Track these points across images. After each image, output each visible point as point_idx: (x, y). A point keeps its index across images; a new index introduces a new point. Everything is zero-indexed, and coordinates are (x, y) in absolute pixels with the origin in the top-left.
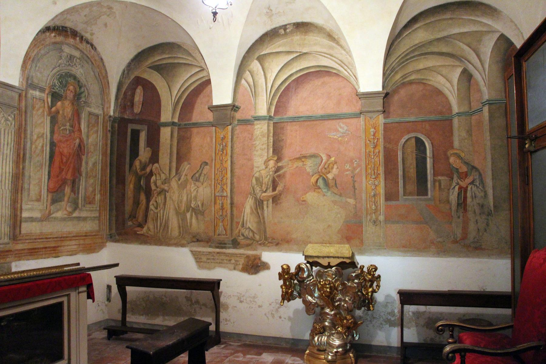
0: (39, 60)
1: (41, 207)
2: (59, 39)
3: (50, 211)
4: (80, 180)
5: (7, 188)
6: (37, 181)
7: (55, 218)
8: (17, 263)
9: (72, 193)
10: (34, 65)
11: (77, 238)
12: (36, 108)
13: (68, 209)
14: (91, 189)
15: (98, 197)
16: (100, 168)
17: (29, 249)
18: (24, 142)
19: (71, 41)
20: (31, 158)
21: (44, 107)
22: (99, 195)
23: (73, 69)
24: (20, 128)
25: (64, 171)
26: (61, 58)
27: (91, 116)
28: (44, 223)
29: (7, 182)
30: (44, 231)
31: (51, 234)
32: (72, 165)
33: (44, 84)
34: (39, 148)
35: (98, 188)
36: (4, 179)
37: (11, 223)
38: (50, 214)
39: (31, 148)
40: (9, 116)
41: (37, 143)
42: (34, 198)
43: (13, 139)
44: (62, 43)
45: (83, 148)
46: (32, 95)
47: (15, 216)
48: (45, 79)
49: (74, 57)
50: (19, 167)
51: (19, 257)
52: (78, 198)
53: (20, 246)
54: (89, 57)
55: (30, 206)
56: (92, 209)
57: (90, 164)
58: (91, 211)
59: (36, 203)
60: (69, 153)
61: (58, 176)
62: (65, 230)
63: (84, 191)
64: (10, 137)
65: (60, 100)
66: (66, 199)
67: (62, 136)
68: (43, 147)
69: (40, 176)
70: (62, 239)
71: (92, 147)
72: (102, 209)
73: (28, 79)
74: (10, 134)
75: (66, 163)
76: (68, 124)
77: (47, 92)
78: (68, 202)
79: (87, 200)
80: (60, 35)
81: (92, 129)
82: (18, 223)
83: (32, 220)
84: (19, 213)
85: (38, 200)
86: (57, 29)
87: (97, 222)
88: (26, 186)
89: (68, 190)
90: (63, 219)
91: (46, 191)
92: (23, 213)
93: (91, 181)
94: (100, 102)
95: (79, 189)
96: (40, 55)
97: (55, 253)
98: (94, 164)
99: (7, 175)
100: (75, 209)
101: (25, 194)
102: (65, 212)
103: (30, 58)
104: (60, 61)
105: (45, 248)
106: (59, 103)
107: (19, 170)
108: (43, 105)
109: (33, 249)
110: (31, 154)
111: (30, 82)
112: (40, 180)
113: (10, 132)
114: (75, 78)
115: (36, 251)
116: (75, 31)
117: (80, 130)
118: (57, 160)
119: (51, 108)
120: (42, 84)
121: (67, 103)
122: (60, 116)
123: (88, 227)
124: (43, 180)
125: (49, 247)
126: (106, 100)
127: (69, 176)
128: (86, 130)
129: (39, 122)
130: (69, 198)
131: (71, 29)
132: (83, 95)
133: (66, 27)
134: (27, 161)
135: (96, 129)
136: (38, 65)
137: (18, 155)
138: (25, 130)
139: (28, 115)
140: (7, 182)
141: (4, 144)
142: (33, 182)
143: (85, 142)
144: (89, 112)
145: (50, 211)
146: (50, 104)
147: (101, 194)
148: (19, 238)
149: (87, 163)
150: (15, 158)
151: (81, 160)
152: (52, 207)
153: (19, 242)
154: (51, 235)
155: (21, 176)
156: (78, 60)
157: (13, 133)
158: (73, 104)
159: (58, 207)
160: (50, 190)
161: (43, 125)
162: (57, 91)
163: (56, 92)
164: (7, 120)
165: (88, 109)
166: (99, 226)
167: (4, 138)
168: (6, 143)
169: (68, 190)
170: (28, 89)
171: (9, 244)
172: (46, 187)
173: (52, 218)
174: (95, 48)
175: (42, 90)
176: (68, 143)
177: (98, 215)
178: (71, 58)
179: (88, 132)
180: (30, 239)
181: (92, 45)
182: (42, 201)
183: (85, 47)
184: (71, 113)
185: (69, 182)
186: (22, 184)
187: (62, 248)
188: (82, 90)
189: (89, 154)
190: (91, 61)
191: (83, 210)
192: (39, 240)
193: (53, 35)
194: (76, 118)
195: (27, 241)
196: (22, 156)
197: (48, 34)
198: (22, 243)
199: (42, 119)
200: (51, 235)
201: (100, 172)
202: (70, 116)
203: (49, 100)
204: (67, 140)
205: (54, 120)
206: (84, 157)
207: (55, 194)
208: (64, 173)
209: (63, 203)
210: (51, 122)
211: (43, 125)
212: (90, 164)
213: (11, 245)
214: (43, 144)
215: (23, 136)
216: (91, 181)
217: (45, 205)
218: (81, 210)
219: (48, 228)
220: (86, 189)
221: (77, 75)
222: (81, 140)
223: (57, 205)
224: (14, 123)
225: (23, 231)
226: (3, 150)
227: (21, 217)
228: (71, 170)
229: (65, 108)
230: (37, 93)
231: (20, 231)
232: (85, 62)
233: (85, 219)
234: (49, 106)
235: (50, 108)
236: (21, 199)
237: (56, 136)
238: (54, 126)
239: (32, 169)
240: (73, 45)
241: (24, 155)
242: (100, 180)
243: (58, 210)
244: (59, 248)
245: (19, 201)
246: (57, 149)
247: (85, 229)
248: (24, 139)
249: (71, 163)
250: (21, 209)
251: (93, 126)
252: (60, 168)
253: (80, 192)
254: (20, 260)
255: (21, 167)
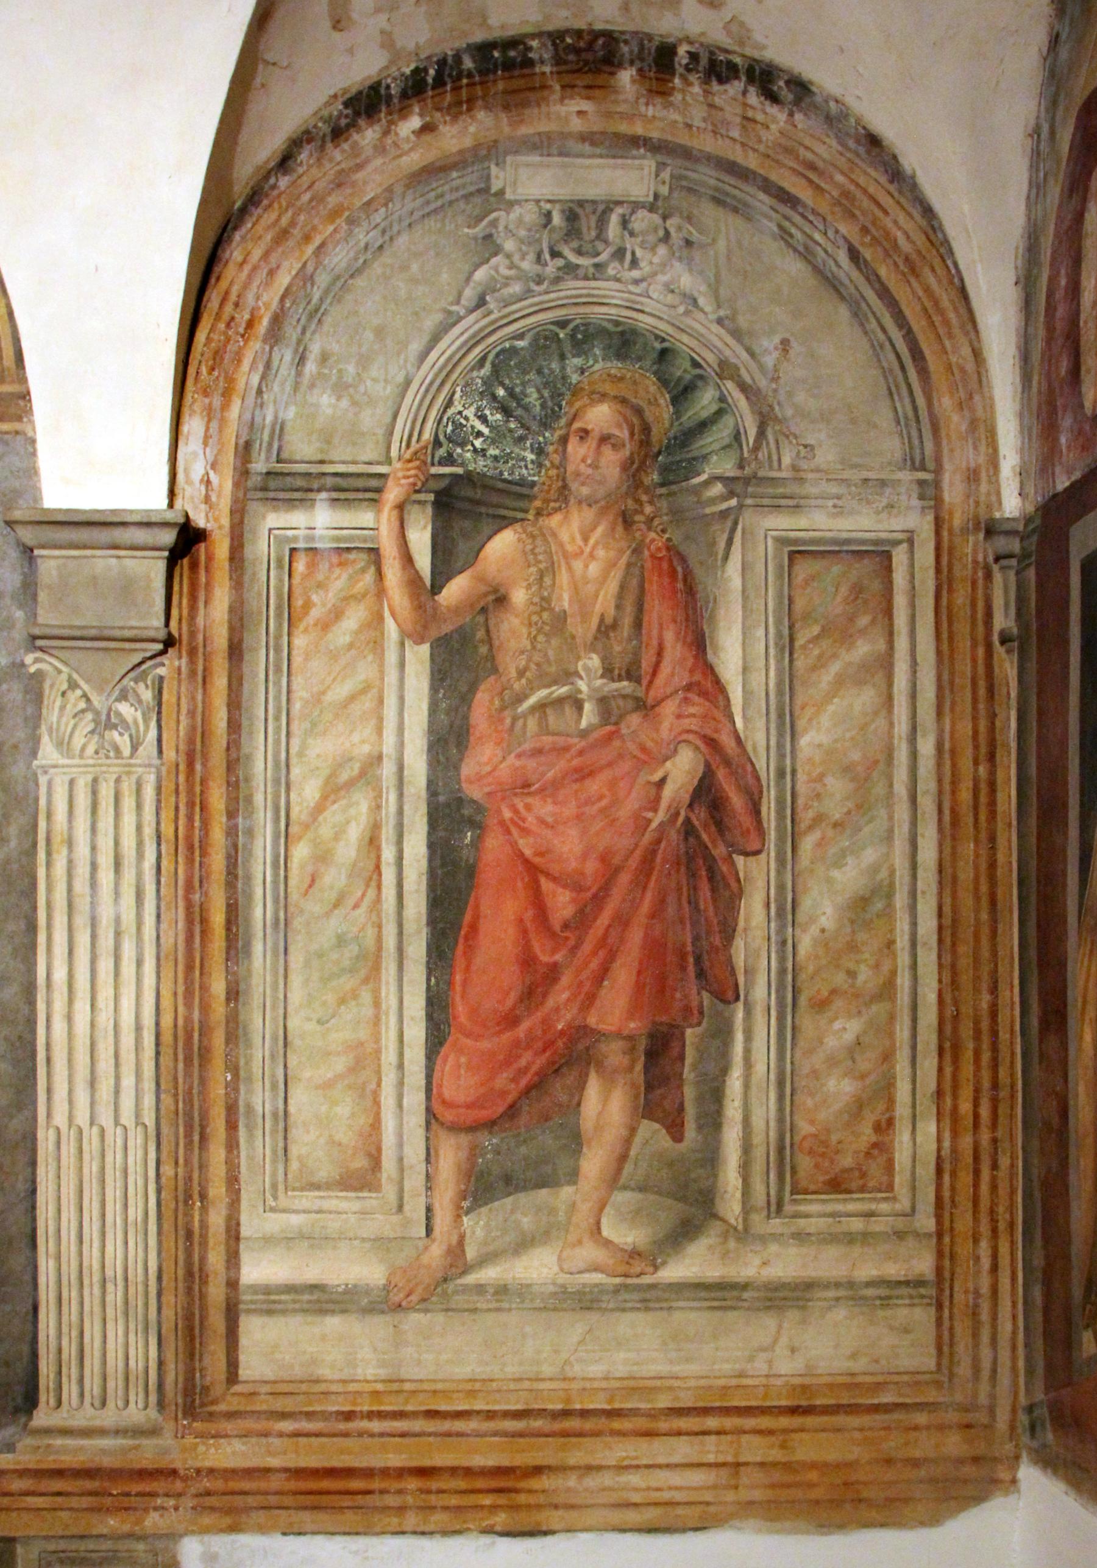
0: (316, 315)
1: (383, 1224)
2: (455, 136)
3: (457, 1250)
4: (722, 1033)
5: (127, 1117)
6: (340, 1064)
7: (502, 1290)
8: (221, 1543)
9: (648, 1128)
10: (285, 356)
11: (712, 1423)
12: (315, 613)
13: (605, 1233)
14: (840, 1088)
15: (917, 1142)
16: (928, 925)
17: (298, 1473)
18: (232, 832)
19: (570, 112)
20: (283, 924)
21: (381, 592)
22: (929, 1128)
23: (602, 287)
24: (194, 753)
25: (586, 982)
26: (489, 245)
27: (804, 569)
28: (415, 1318)
29: (128, 1081)
30: (410, 1372)
31: (473, 1387)
32: (636, 937)
33: (370, 451)
34: (348, 849)
35: (914, 1079)
36: (105, 1065)
37: (168, 1313)
38: (457, 1261)
39: (281, 863)
40: (123, 697)
41: (325, 831)
42: (325, 1172)
43: (149, 831)
44: (487, 152)
45: (737, 801)
46: (282, 541)
47: (194, 1277)
48: (371, 419)
49: (610, 205)
50: (204, 988)
51: (229, 1511)
52: (711, 1158)
53: (230, 1452)
54: (752, 162)
55: (295, 1220)
56: (857, 1225)
57: (822, 912)
58: (865, 1238)
59: (345, 1203)
60: (604, 859)
61: (511, 1020)
62: (596, 1370)
63: (765, 1112)
64: (129, 820)
65: (504, 522)
66: (593, 1163)
67: (538, 752)
68: (373, 842)
69: (363, 1034)
70: (574, 1424)
71: (837, 786)
72: (964, 1223)
73: (245, 451)
74: (128, 803)
75: (582, 920)
76: (594, 661)
77: (393, 494)
78: (613, 1180)
79: (805, 1163)
80: (461, 108)
81: (820, 664)
82: (217, 1321)
83: (319, 1300)
84: (216, 1259)
85: (361, 1178)
86: (439, 82)
87: (922, 1317)
88: (259, 1098)
89: (604, 1106)
90: (585, 1301)
91: (415, 1119)
92: (245, 1257)
93: (844, 1029)
94: (892, 446)
95: (714, 1095)
96: (323, 279)
97: (515, 1508)
98: (867, 907)
99: (128, 1040)
100: (683, 1233)
101: (257, 1147)
102: (589, 1252)
103: (250, 324)
104: (480, 275)
105: (423, 1472)
106: (502, 545)
107: (205, 1008)
108: (369, 577)
109: (331, 1472)
110: (283, 901)
111: (259, 465)
112: (364, 1059)
113: (127, 787)
114: (623, 341)
115: (356, 1484)
116: (596, 35)
117: (708, 686)
118: (499, 918)
119: (436, 588)
120: (353, 457)
121: (568, 528)
122: (512, 631)
123: (823, 1347)
124: (389, 1057)
125: (468, 1472)
126: (955, 422)
127: (615, 1010)
128: (766, 678)
129: (341, 691)
130: (623, 1158)
131: (556, 37)
132: (721, 433)
133: (513, 43)
134: (258, 948)
135: (863, 649)
136: (315, 349)
137: (196, 919)
138: (235, 762)
139: (257, 662)
140: (128, 1081)
141: (94, 866)
142: (308, 1074)
143: (763, 763)
144: (781, 541)
145: (457, 1250)
146: (424, 562)
147: (950, 1119)
148: (222, 1407)
149: (786, 909)
150: (174, 934)
151: (727, 893)
152: (478, 1227)
153: (228, 1426)
154: (471, 1394)
155: (218, 1040)
156: (642, 220)
157: (149, 792)
158: (627, 521)
159: (526, 1222)
160: (448, 1116)
161: (367, 703)
162: (480, 465)
163: (469, 478)
164: (107, 723)
165: (781, 523)
166: (944, 1346)
167: (94, 830)
168: (105, 860)
169: (604, 1106)
170: (254, 507)
171: (153, 1432)
172: (415, 1099)
173: (480, 1289)
174: (801, 88)
175: (357, 489)
176: (594, 786)
177: (924, 1264)
178: (579, 221)
179: (789, 683)
180: (309, 1415)
181: (764, 78)
182: (389, 1192)
183: (698, 115)
184: (612, 586)
185: (614, 1053)
186: (233, 1087)
187: (572, 1481)
188: (705, 401)
189: (807, 844)
190: (767, 186)
191: (763, 1239)
192: (376, 1426)
193: (415, 122)
194: (657, 610)
195: (287, 1426)
196: (218, 919)
197: (368, 136)
198: (245, 1435)
199: (365, 671)
200: (471, 1394)
201: (928, 959)
202: (605, 602)
203: (421, 539)
204: (583, 774)
205: (460, 659)
206: (757, 875)
207: (489, 1141)
208: (560, 995)
209: (567, 1192)
210: (440, 677)
211: (367, 703)
212: (822, 912)
213: (167, 1440)
214: (376, 827)
215: (217, 800)
216: (844, 1029)
217: (416, 1209)
218: (744, 1234)
219: (445, 1354)
220: (786, 1085)
221: (645, 321)
222: (721, 757)
223: (520, 1210)
224: (153, 733)
225: (254, 1365)
226: (93, 905)
227: (233, 1284)
228: (623, 977)
229: (566, 563)
230: (320, 520)
231: (233, 1365)
232: (708, 213)
233: (787, 1297)
234: (414, 581)
235: (425, 592)
236: (233, 1181)
237: (483, 764)
238: (466, 699)
239: (296, 996)
240: (585, 138)
241: (234, 913)
242: (929, 1016)
243: (524, 1244)
244: (544, 1482)
245: (217, 1190)
246: (494, 843)
247: (787, 1366)
248: (231, 814)
249: (622, 921)
250: (233, 1234)
251: (841, 632)
252: (527, 961)
253: (733, 1110)
254: (234, 1529)
255: (218, 987)
